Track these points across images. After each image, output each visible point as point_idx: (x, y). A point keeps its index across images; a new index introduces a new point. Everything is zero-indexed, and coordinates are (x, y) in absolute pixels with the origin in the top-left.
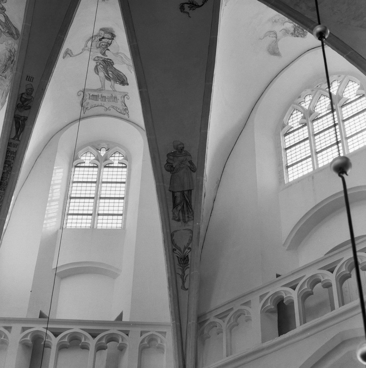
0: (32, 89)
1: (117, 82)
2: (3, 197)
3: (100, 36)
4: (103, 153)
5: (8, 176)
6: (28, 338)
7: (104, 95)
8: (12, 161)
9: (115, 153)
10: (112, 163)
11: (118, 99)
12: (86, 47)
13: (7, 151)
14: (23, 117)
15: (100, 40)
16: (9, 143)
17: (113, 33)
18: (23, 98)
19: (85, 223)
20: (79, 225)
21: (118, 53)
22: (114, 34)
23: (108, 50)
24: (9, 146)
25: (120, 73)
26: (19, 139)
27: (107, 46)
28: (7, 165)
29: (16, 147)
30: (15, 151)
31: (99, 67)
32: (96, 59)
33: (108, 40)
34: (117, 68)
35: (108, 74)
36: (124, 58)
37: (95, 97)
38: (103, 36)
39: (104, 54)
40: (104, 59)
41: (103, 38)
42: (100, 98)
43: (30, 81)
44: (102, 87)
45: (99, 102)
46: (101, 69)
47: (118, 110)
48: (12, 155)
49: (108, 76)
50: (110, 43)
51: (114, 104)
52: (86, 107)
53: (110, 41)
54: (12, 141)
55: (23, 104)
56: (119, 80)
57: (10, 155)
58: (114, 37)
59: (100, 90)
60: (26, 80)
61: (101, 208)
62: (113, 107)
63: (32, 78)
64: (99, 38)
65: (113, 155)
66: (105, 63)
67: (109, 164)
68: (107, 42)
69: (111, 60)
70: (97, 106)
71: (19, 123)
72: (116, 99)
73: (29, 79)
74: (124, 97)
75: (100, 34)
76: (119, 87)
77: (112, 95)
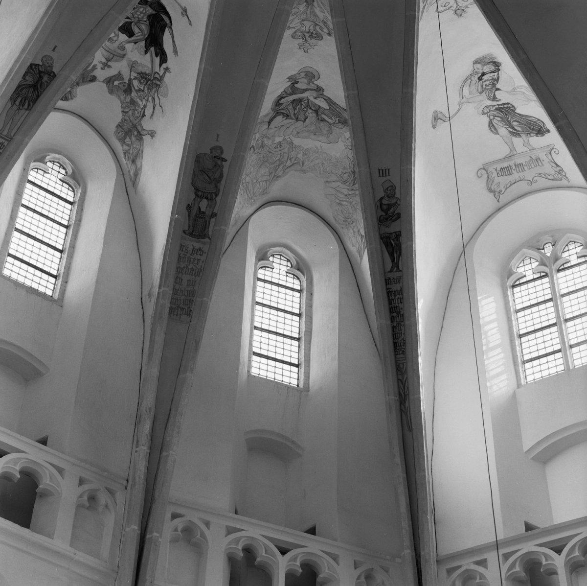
0: (393, 187)
1: (532, 135)
2: (404, 364)
3: (477, 73)
4: (548, 251)
5: (401, 330)
6: (518, 568)
7: (518, 161)
8: (401, 305)
9: (567, 245)
10: (568, 261)
11: (543, 161)
13: (388, 293)
14: (394, 234)
15: (480, 79)
16: (386, 280)
17: (495, 60)
18: (385, 205)
19: (554, 366)
20: (545, 373)
21: (514, 89)
23: (498, 89)
24: (389, 284)
25: (530, 119)
26: (399, 269)
28: (395, 314)
29: (399, 281)
30: (399, 289)
31: (495, 122)
32: (486, 111)
33: (494, 74)
35: (513, 127)
36: (526, 92)
37: (505, 171)
38: (481, 71)
39: (494, 98)
40: (497, 106)
41: (483, 74)
42: (514, 169)
43: (386, 176)
44: (511, 151)
45: (516, 176)
46: (499, 124)
47: (549, 177)
48: (397, 297)
49: (514, 131)
50: (496, 78)
51: (539, 170)
52: (498, 190)
53: (496, 74)
54: (390, 275)
55: (387, 214)
56: (533, 129)
57: (393, 297)
58: (499, 66)
59: (509, 157)
60: (380, 176)
61: (571, 336)
62: (540, 175)
63: (387, 170)
64: (477, 77)
65: (566, 249)
66: (502, 112)
67: (563, 265)
68: (491, 78)
69: (508, 104)
70: (514, 183)
71: (392, 244)
72: (539, 161)
73: (383, 173)
74: (550, 154)
75: (477, 70)
76: (537, 141)
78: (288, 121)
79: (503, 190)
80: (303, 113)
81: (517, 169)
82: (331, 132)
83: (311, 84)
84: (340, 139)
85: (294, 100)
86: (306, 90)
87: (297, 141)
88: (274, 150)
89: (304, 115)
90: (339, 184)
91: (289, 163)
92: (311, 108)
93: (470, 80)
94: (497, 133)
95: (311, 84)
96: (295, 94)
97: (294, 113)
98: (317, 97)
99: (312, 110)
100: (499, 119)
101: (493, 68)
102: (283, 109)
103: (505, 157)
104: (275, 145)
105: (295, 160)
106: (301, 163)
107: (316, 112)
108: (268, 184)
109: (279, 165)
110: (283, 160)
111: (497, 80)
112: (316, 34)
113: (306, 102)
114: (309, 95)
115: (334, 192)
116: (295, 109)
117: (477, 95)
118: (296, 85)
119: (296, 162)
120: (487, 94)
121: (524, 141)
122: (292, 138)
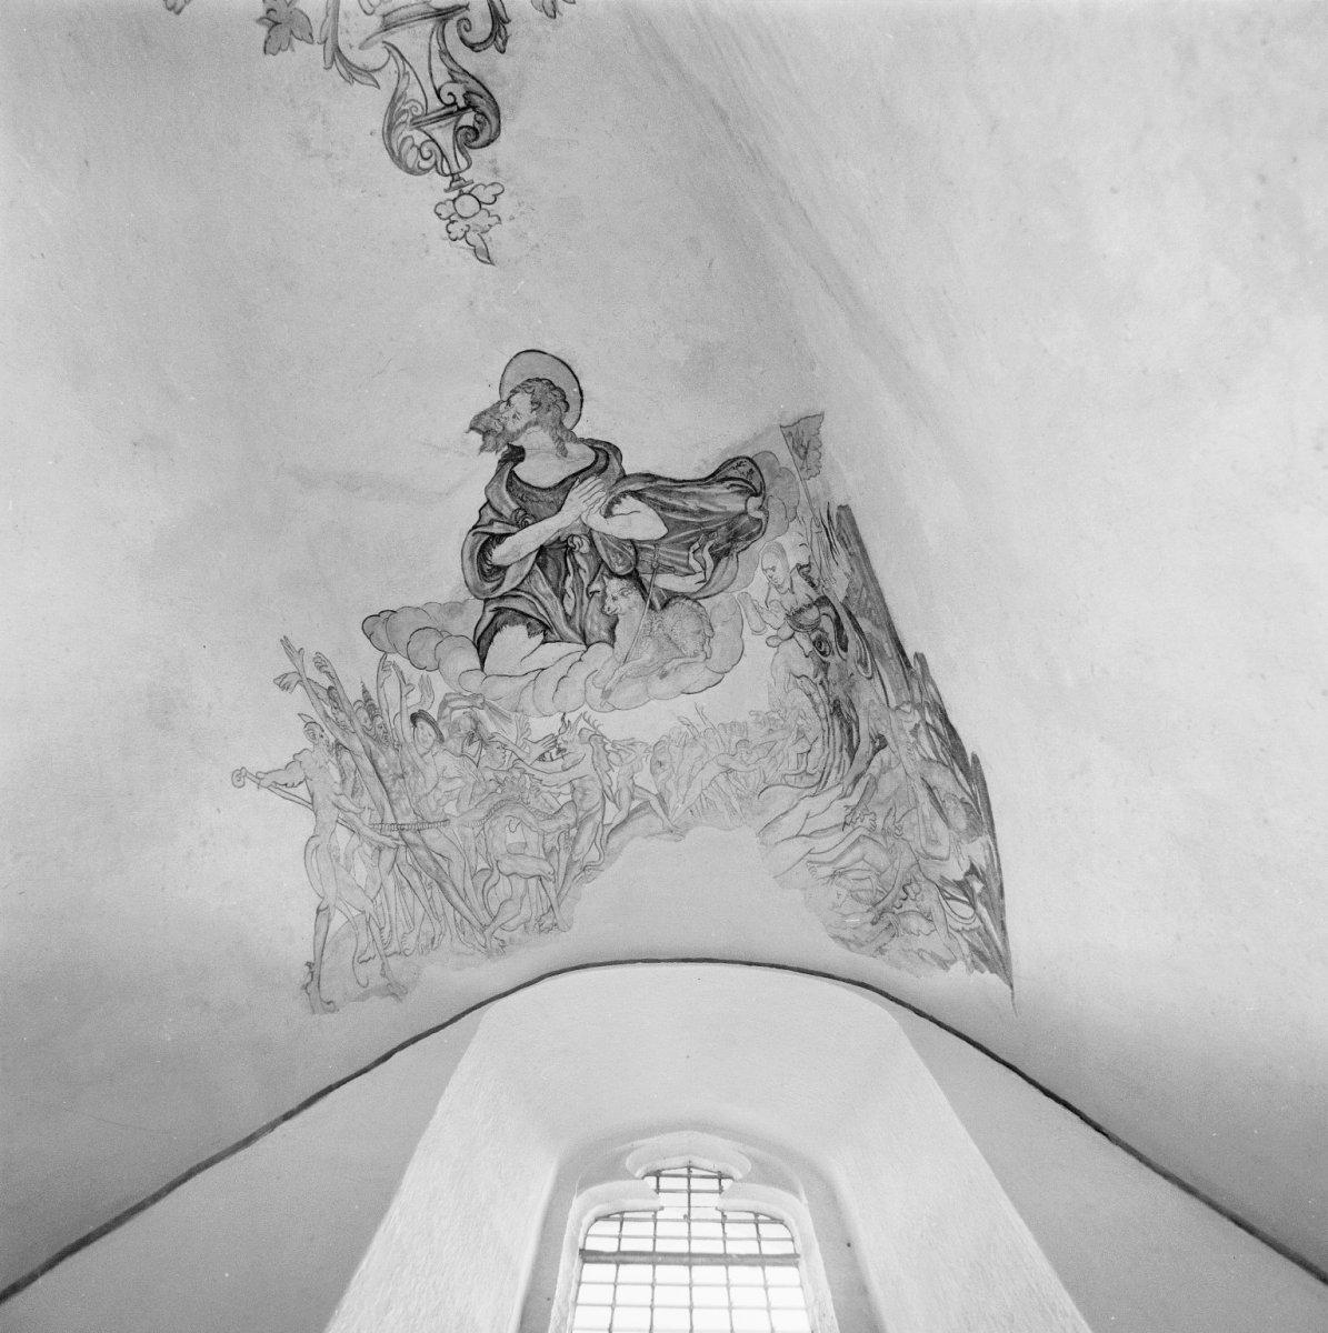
78: (553, 651)
80: (595, 605)
82: (708, 633)
83: (570, 447)
84: (747, 629)
85: (542, 550)
86: (565, 486)
87: (614, 725)
88: (539, 765)
89: (602, 611)
90: (804, 806)
91: (612, 815)
92: (613, 574)
95: (572, 448)
96: (537, 520)
97: (566, 614)
98: (611, 504)
99: (619, 577)
102: (515, 593)
104: (539, 750)
105: (632, 798)
106: (655, 803)
107: (634, 577)
108: (553, 895)
109: (579, 824)
110: (586, 805)
112: (470, 106)
113: (585, 548)
114: (582, 507)
115: (797, 848)
116: (562, 596)
118: (522, 470)
119: (635, 804)
122: (595, 716)
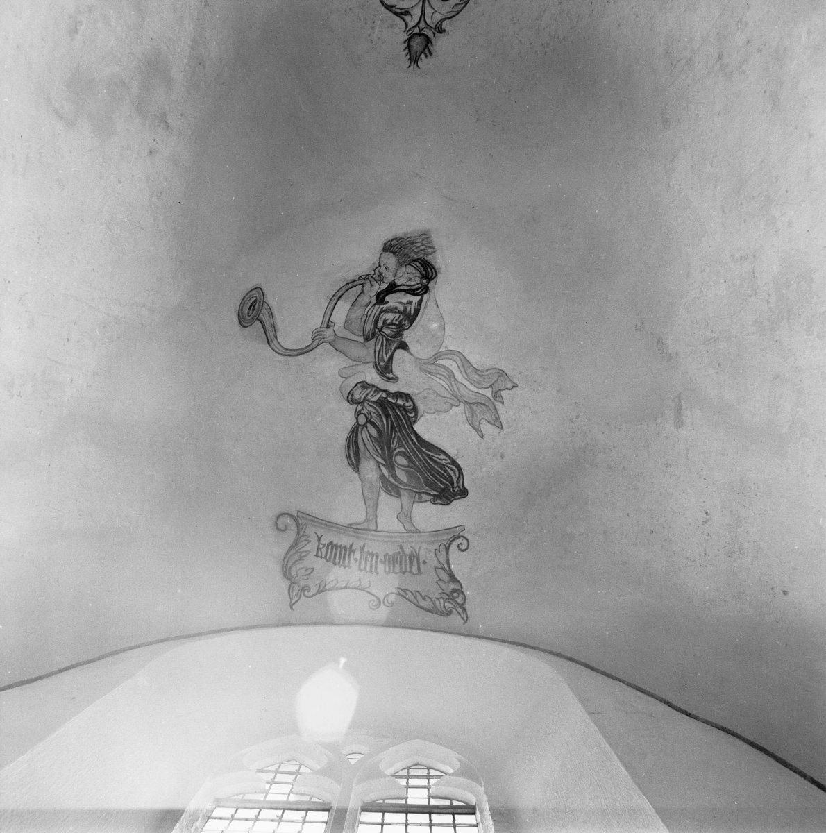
1: (425, 497)
3: (381, 278)
11: (425, 562)
12: (328, 326)
15: (380, 298)
17: (429, 258)
21: (438, 356)
22: (431, 266)
23: (404, 346)
27: (400, 328)
31: (363, 435)
32: (358, 394)
34: (427, 437)
36: (458, 375)
38: (391, 279)
39: (385, 370)
40: (384, 395)
44: (367, 520)
47: (423, 603)
49: (392, 480)
50: (412, 312)
52: (303, 583)
53: (416, 299)
58: (430, 279)
64: (377, 288)
66: (387, 416)
68: (401, 308)
69: (407, 397)
70: (342, 588)
72: (415, 563)
74: (447, 549)
75: (383, 270)
77: (401, 548)
79: (314, 590)
81: (363, 562)
93: (358, 289)
94: (355, 465)
100: (374, 433)
101: (416, 280)
103: (350, 526)
111: (410, 317)
117: (355, 338)
120: (378, 349)
121: (402, 508)
